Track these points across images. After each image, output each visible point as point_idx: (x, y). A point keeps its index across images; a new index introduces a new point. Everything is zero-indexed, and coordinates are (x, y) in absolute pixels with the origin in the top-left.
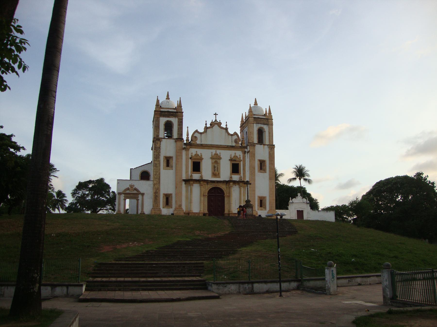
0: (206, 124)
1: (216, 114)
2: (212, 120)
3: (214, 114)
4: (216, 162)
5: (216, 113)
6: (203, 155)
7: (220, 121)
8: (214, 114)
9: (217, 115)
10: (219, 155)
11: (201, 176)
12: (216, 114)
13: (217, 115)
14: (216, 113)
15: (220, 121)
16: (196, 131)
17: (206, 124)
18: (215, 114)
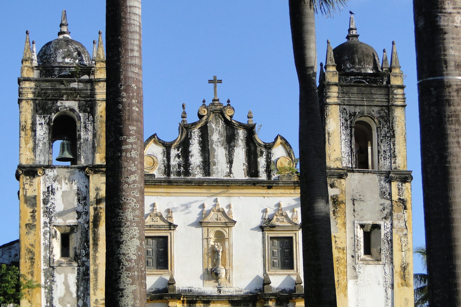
0: (23, 182)
1: (214, 81)
2: (204, 101)
3: (210, 81)
4: (220, 237)
5: (215, 77)
6: (174, 215)
7: (229, 101)
8: (210, 81)
9: (220, 81)
10: (226, 211)
11: (171, 282)
12: (214, 81)
13: (220, 81)
14: (215, 77)
15: (229, 101)
16: (154, 136)
17: (184, 113)
18: (213, 79)
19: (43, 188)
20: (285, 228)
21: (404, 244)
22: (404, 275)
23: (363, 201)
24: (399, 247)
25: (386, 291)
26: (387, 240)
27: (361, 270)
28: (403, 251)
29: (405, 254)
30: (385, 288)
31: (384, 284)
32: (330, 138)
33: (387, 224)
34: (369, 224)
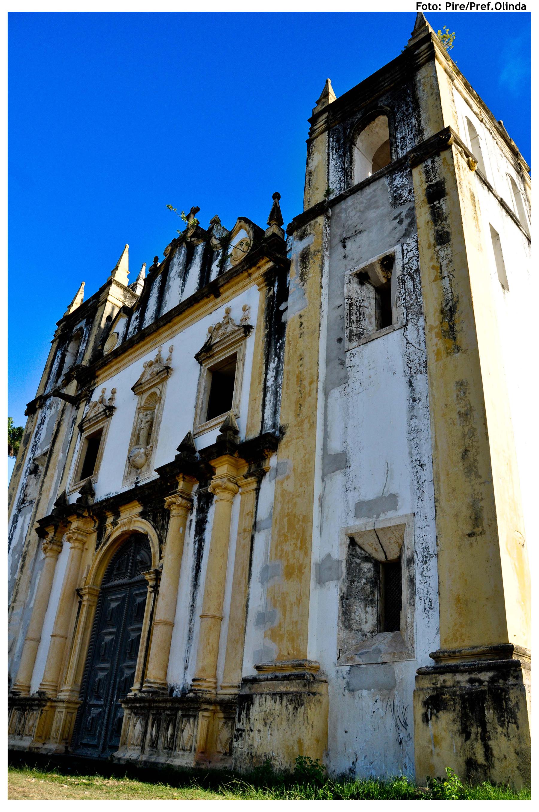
19: (39, 422)
20: (225, 343)
21: (444, 263)
22: (451, 328)
23: (361, 231)
24: (433, 274)
25: (410, 384)
26: (410, 274)
27: (356, 361)
28: (444, 278)
29: (450, 281)
30: (407, 379)
31: (407, 368)
32: (311, 178)
33: (408, 245)
34: (372, 265)
